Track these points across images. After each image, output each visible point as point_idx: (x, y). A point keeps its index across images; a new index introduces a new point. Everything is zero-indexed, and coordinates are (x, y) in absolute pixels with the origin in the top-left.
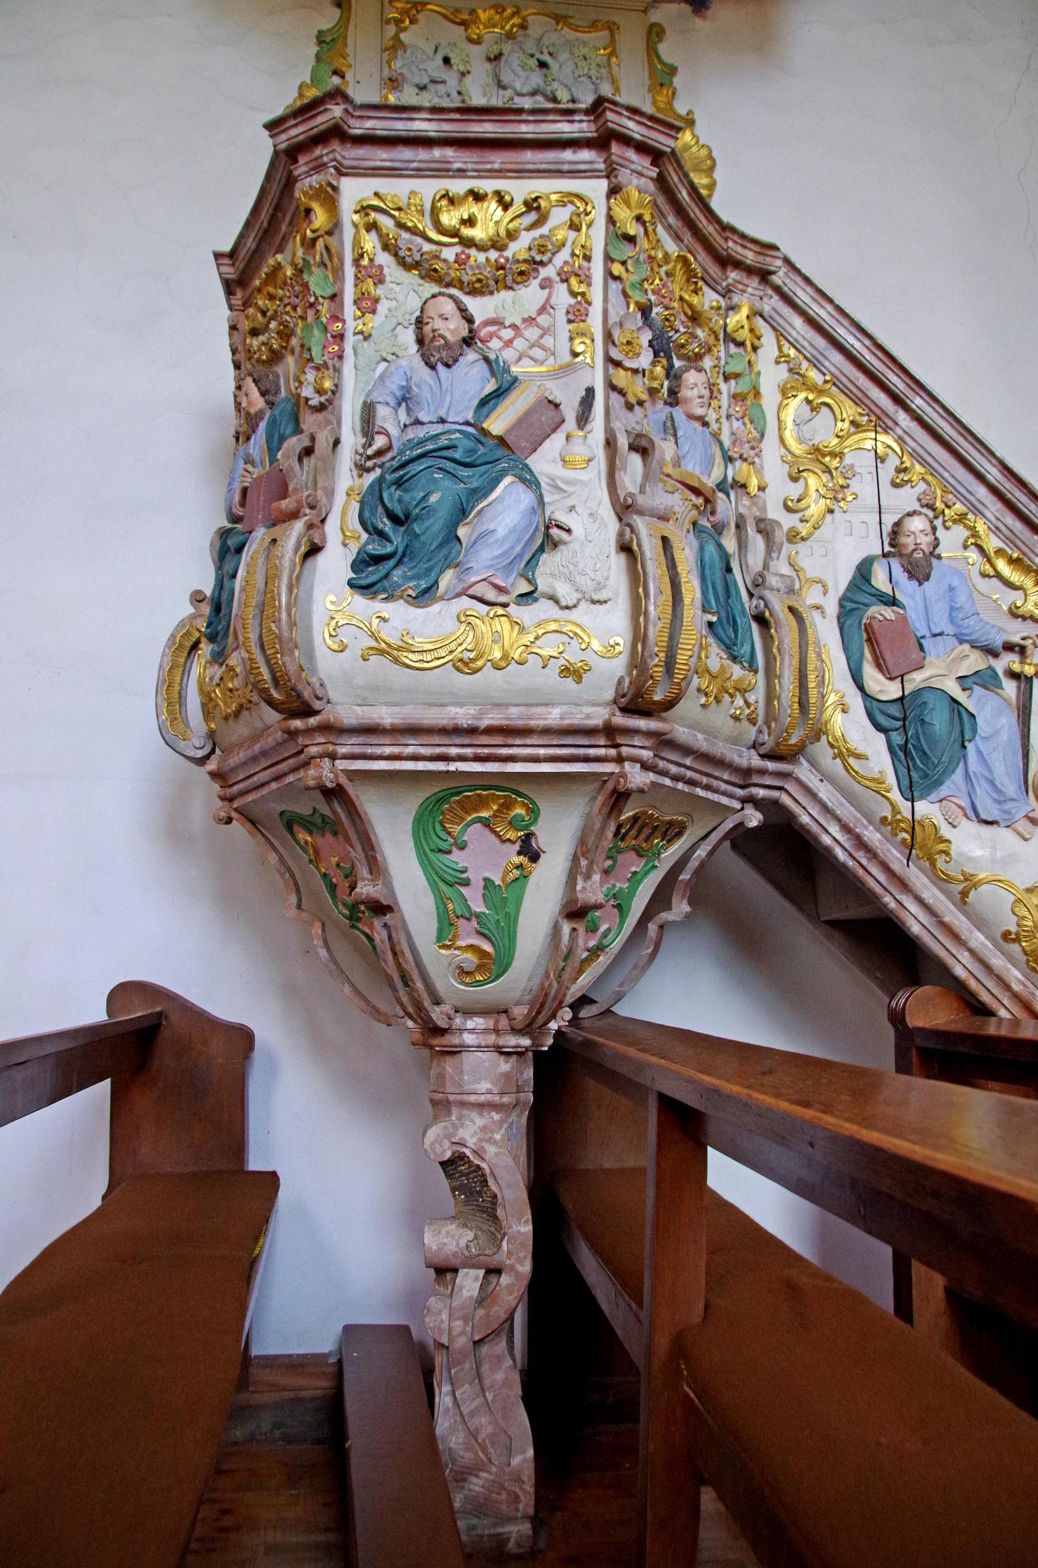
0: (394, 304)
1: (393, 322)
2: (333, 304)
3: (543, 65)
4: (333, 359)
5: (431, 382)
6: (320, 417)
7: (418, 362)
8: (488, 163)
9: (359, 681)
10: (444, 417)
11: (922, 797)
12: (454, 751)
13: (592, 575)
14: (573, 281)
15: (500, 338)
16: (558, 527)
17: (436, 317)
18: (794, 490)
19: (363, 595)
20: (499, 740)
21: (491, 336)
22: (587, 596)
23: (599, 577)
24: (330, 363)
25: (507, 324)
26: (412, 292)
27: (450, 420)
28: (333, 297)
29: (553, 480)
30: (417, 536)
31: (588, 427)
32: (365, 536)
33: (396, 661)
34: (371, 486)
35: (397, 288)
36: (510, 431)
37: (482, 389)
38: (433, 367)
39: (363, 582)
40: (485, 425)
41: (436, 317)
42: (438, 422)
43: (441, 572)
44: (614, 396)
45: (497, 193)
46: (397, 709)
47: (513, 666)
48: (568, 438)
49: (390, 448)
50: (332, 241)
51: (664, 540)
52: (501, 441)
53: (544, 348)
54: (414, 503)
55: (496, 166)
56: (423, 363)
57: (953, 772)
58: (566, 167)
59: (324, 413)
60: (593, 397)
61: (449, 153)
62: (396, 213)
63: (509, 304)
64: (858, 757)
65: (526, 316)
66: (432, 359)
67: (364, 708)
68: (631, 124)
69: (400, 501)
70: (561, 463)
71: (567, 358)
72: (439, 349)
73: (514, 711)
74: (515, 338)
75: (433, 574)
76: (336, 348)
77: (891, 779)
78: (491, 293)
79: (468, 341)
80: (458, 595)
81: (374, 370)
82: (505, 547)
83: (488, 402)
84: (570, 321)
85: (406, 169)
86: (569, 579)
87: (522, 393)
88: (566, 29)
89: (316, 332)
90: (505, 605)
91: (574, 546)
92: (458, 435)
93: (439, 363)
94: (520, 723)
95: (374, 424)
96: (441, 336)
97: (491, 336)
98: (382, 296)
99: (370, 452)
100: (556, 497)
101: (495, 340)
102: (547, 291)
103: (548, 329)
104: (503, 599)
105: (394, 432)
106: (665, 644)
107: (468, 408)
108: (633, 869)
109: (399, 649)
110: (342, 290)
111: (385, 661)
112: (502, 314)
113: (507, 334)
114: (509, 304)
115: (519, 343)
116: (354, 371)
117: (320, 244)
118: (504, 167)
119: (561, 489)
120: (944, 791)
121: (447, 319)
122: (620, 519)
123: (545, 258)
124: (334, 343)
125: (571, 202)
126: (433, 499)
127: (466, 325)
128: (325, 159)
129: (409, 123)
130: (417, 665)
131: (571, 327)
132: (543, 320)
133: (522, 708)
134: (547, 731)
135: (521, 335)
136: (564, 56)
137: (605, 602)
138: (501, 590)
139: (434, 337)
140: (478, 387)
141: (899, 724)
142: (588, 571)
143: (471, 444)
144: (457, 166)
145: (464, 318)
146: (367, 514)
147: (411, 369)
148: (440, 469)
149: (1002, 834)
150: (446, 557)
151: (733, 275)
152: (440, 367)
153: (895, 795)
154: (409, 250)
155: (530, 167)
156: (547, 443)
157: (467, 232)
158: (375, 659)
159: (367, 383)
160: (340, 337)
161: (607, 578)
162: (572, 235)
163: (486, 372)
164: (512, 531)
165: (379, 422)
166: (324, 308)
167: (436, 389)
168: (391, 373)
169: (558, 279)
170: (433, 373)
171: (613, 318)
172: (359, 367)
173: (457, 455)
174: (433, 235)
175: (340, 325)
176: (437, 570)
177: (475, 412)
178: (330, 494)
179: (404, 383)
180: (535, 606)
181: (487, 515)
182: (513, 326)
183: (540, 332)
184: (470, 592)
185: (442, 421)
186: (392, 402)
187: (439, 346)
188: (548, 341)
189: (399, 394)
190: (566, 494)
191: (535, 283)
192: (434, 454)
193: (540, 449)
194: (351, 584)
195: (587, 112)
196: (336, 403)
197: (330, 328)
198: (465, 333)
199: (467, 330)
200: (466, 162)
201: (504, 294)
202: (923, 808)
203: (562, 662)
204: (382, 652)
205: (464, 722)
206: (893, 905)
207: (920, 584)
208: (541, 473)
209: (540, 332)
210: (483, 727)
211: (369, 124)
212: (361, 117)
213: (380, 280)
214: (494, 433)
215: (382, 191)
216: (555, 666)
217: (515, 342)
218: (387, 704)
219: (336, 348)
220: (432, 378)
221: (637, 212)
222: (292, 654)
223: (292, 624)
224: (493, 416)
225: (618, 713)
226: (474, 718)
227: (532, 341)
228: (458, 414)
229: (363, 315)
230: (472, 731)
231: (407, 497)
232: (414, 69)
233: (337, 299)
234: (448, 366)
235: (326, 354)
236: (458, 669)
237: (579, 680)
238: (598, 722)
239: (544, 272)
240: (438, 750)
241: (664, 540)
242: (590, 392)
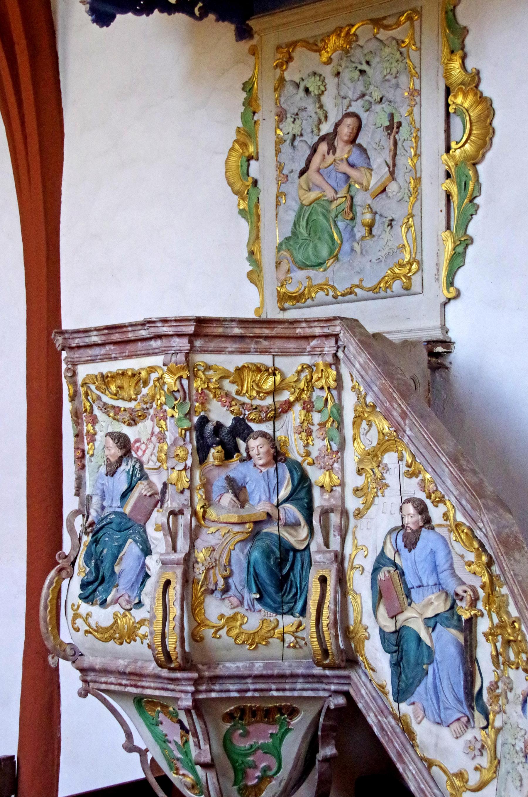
3: (362, 72)
11: (402, 701)
12: (124, 682)
18: (360, 481)
20: (137, 678)
21: (138, 448)
35: (104, 424)
55: (127, 354)
57: (418, 686)
58: (151, 352)
61: (112, 347)
64: (373, 670)
73: (139, 664)
77: (389, 688)
83: (125, 496)
88: (382, 30)
106: (160, 643)
108: (270, 732)
115: (148, 452)
120: (412, 699)
123: (148, 406)
126: (105, 551)
136: (374, 61)
141: (396, 648)
144: (114, 355)
149: (445, 733)
151: (314, 343)
153: (391, 697)
194: (80, 597)
202: (405, 708)
205: (121, 669)
206: (401, 770)
207: (410, 551)
211: (77, 341)
226: (126, 667)
232: (289, 103)
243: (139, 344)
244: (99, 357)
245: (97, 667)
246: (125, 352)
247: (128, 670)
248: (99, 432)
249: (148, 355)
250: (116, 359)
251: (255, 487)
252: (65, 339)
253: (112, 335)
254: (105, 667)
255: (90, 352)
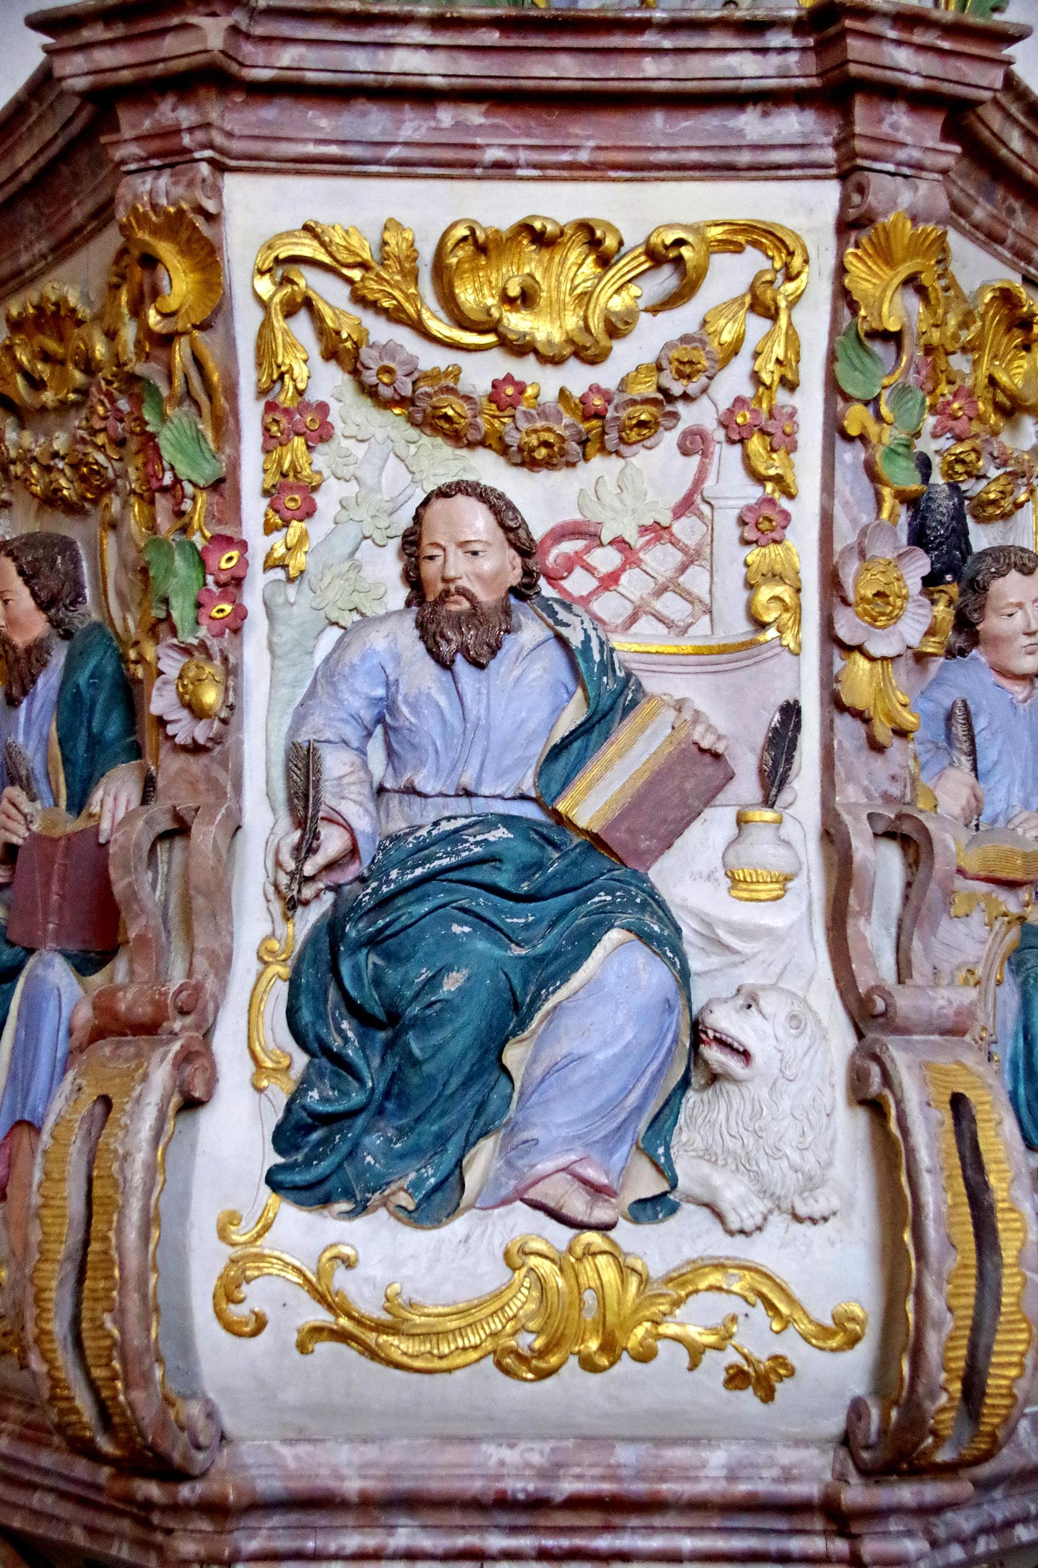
0: (353, 487)
1: (352, 532)
2: (216, 498)
4: (221, 634)
5: (443, 701)
6: (196, 765)
7: (407, 633)
8: (565, 148)
9: (291, 1396)
10: (472, 788)
13: (795, 1157)
14: (756, 444)
15: (589, 569)
16: (723, 1043)
17: (452, 548)
19: (299, 1203)
20: (594, 1519)
21: (571, 563)
22: (786, 1205)
23: (810, 1164)
24: (214, 645)
25: (606, 537)
26: (392, 461)
27: (485, 790)
28: (216, 486)
29: (709, 925)
30: (416, 1063)
31: (785, 797)
32: (301, 1060)
33: (373, 1354)
34: (312, 940)
35: (359, 451)
36: (614, 825)
37: (557, 711)
38: (445, 664)
39: (299, 1178)
40: (561, 807)
41: (452, 548)
42: (457, 795)
43: (469, 1144)
44: (844, 723)
45: (585, 227)
46: (371, 1452)
47: (626, 1365)
48: (741, 821)
49: (353, 852)
50: (209, 344)
51: (958, 1103)
52: (596, 842)
53: (687, 596)
54: (409, 994)
55: (584, 157)
56: (421, 647)
58: (745, 158)
59: (204, 760)
60: (798, 727)
61: (474, 115)
62: (356, 274)
63: (610, 487)
65: (648, 521)
66: (444, 648)
67: (303, 1449)
68: (902, 57)
69: (378, 982)
70: (727, 882)
71: (739, 628)
72: (458, 621)
73: (625, 1455)
74: (622, 569)
75: (452, 1149)
76: (228, 608)
78: (571, 465)
79: (523, 591)
80: (505, 1202)
81: (311, 653)
82: (610, 1089)
84: (746, 542)
85: (377, 162)
86: (744, 1165)
87: (642, 729)
89: (179, 562)
90: (605, 1228)
91: (757, 1089)
92: (501, 833)
93: (459, 657)
94: (639, 1488)
95: (317, 802)
96: (463, 592)
97: (571, 563)
98: (326, 473)
99: (309, 868)
100: (715, 961)
101: (578, 571)
102: (696, 460)
103: (698, 554)
104: (602, 1214)
105: (362, 824)
107: (521, 762)
109: (381, 1328)
110: (235, 465)
111: (348, 1353)
112: (595, 514)
113: (606, 559)
114: (610, 487)
115: (633, 584)
116: (267, 657)
117: (181, 352)
118: (602, 157)
119: (728, 948)
121: (475, 553)
122: (860, 1035)
123: (692, 388)
124: (224, 597)
125: (755, 244)
126: (451, 984)
127: (518, 560)
128: (187, 140)
129: (381, 54)
130: (418, 1364)
131: (753, 554)
132: (687, 529)
133: (642, 1449)
134: (698, 1506)
135: (637, 563)
137: (825, 1219)
138: (597, 1191)
139: (447, 593)
140: (542, 714)
142: (788, 1151)
143: (527, 852)
144: (492, 155)
145: (512, 545)
146: (306, 1016)
147: (397, 658)
148: (463, 910)
150: (481, 1108)
152: (461, 665)
154: (389, 371)
155: (662, 157)
156: (694, 832)
157: (517, 322)
158: (324, 1348)
159: (295, 684)
160: (235, 582)
161: (829, 1164)
162: (757, 326)
163: (565, 675)
164: (618, 1059)
165: (328, 798)
166: (199, 506)
167: (453, 717)
168: (353, 667)
169: (720, 434)
170: (449, 673)
171: (845, 536)
172: (279, 651)
173: (503, 880)
174: (440, 327)
175: (235, 554)
176: (458, 1139)
177: (539, 774)
178: (223, 964)
179: (380, 692)
180: (673, 1222)
181: (569, 1021)
182: (620, 543)
183: (679, 557)
184: (531, 1194)
185: (468, 794)
186: (352, 733)
187: (459, 615)
188: (696, 580)
189: (368, 715)
190: (736, 958)
191: (669, 439)
192: (451, 875)
193: (679, 842)
194: (274, 1181)
195: (799, 27)
196: (230, 741)
197: (211, 562)
198: (515, 577)
199: (519, 571)
200: (513, 147)
201: (598, 464)
203: (732, 1357)
204: (342, 1336)
205: (520, 1486)
208: (683, 907)
209: (679, 557)
210: (559, 1498)
211: (288, 56)
212: (268, 40)
213: (323, 434)
214: (582, 823)
215: (322, 217)
216: (716, 1365)
217: (624, 579)
218: (350, 1440)
219: (228, 608)
220: (444, 690)
221: (904, 271)
222: (147, 1377)
223: (150, 1308)
224: (580, 783)
225: (854, 1479)
226: (543, 1474)
227: (661, 580)
228: (502, 774)
229: (286, 524)
230: (538, 1504)
231: (393, 977)
233: (226, 487)
234: (479, 665)
235: (204, 620)
236: (506, 1371)
237: (768, 1395)
238: (808, 1489)
239: (689, 415)
240: (462, 1541)
241: (958, 1103)
242: (791, 712)
243: (658, 119)
244: (393, 153)
245: (352, 1486)
246: (577, 148)
247: (567, 1487)
248: (332, 481)
249: (728, 170)
250: (503, 170)
251: (1000, 753)
252: (234, 30)
253: (534, 58)
254: (405, 1485)
255: (323, 123)
